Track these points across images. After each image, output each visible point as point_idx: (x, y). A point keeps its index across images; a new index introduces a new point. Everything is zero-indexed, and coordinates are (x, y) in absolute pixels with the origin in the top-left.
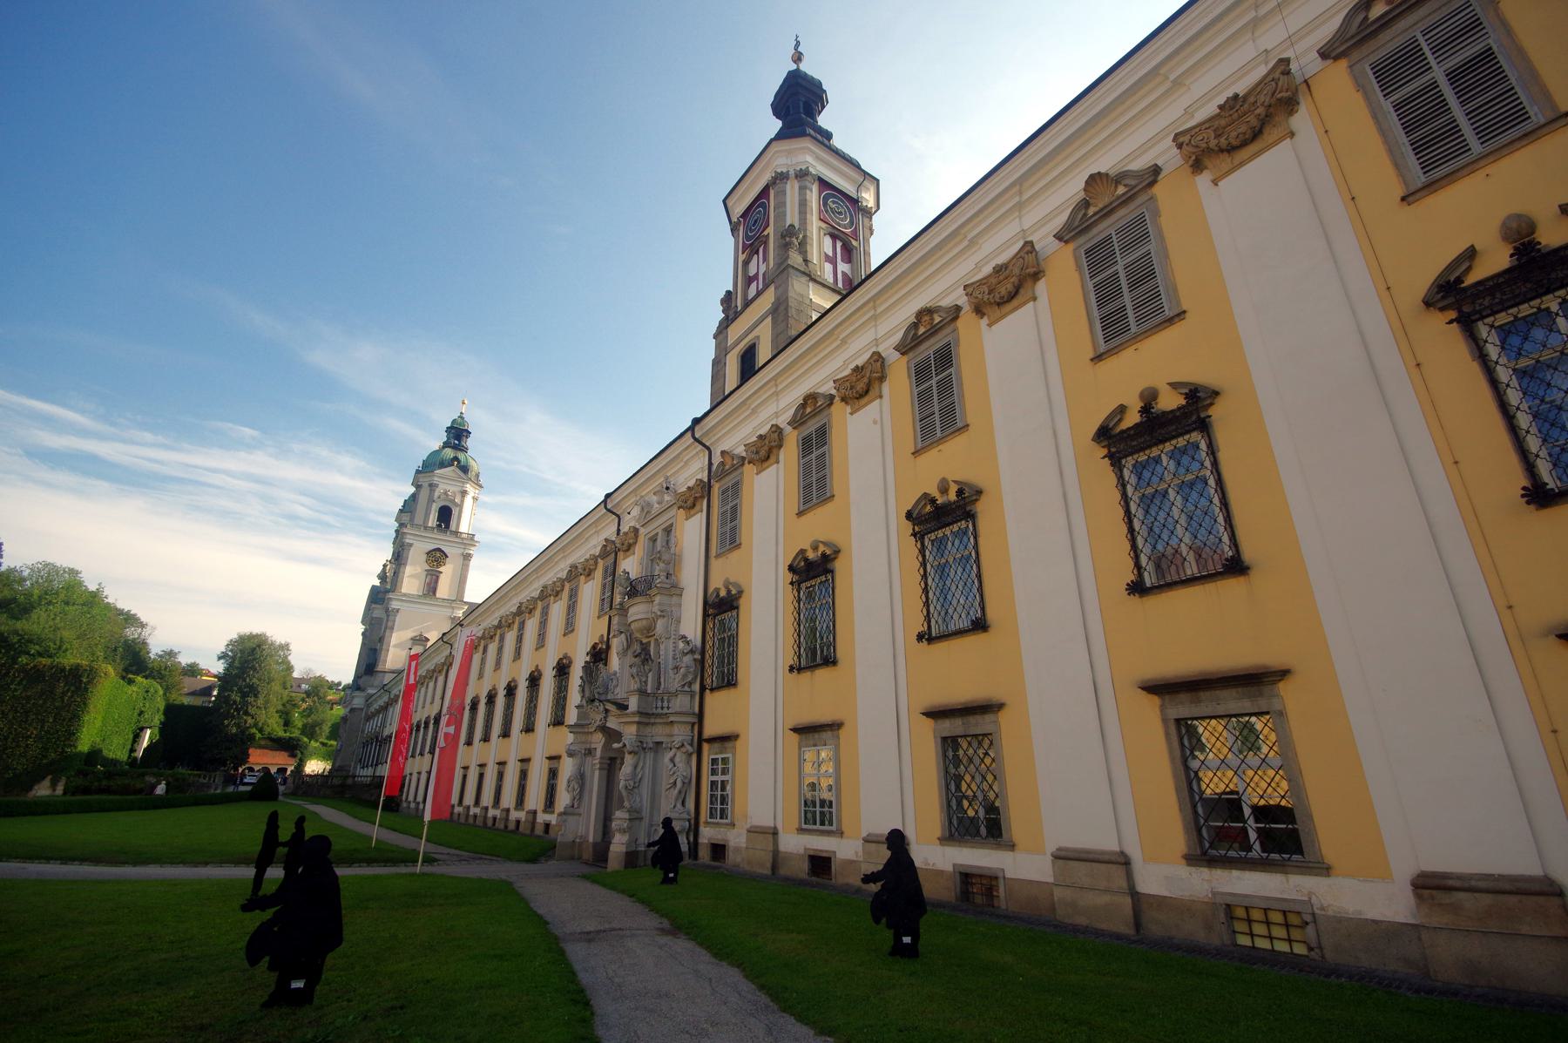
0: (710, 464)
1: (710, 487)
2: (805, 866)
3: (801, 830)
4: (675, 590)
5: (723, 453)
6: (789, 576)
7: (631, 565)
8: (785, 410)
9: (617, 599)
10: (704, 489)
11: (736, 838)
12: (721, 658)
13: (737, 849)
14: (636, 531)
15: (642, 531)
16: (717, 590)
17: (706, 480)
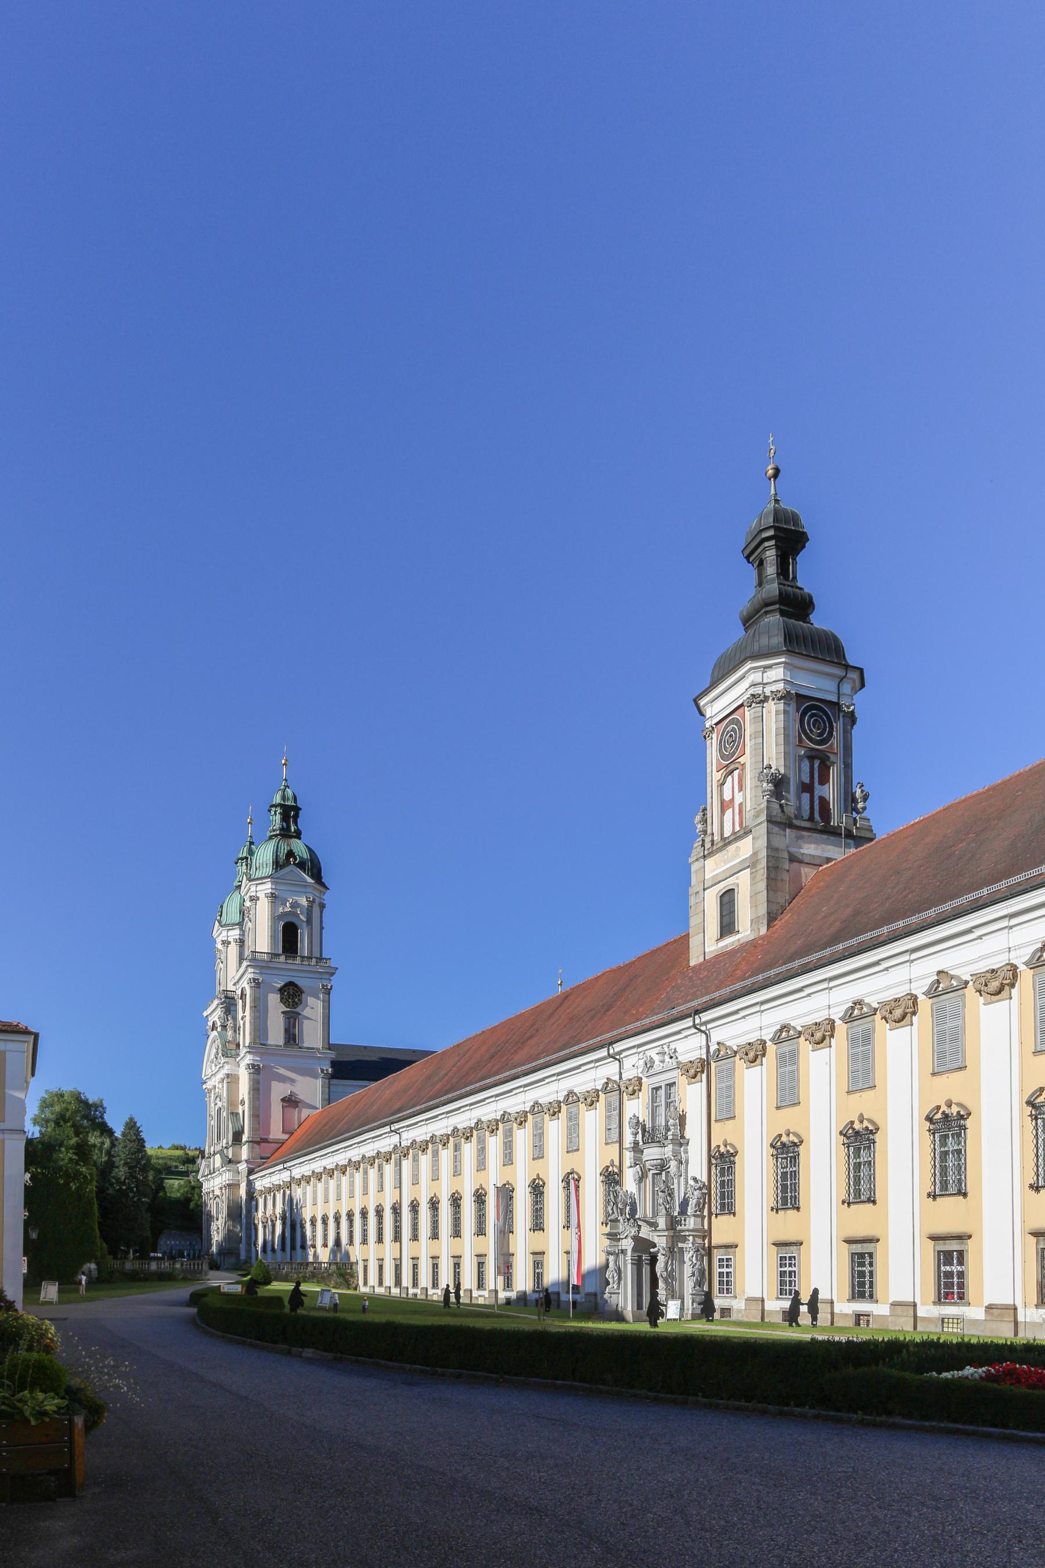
0: (708, 1047)
1: (709, 1064)
2: (781, 1316)
3: (777, 1298)
4: (681, 1141)
5: (718, 1043)
6: (772, 1151)
7: (636, 1108)
8: (768, 1026)
9: (628, 1139)
10: (704, 1065)
11: (738, 1305)
12: (723, 1194)
13: (739, 1311)
14: (640, 1079)
15: (644, 1080)
16: (719, 1146)
17: (704, 1057)
